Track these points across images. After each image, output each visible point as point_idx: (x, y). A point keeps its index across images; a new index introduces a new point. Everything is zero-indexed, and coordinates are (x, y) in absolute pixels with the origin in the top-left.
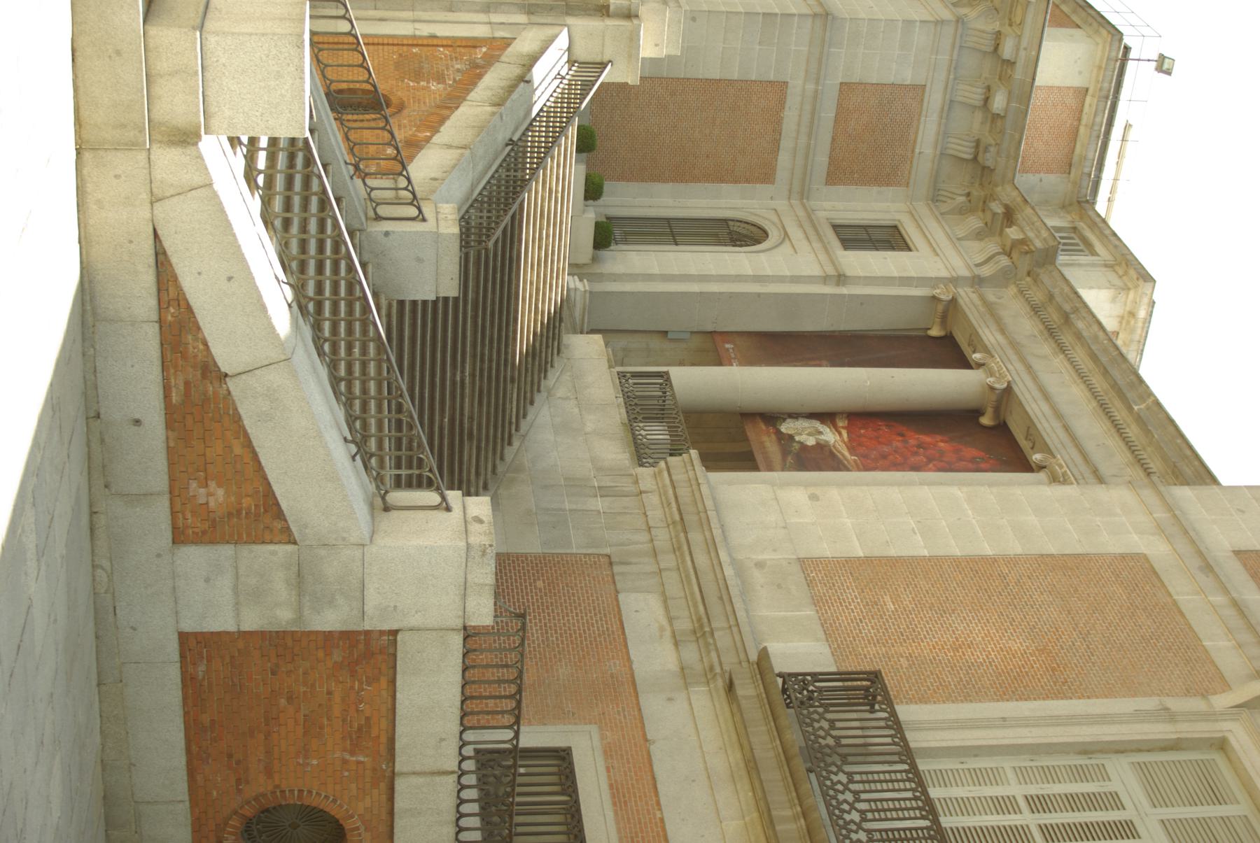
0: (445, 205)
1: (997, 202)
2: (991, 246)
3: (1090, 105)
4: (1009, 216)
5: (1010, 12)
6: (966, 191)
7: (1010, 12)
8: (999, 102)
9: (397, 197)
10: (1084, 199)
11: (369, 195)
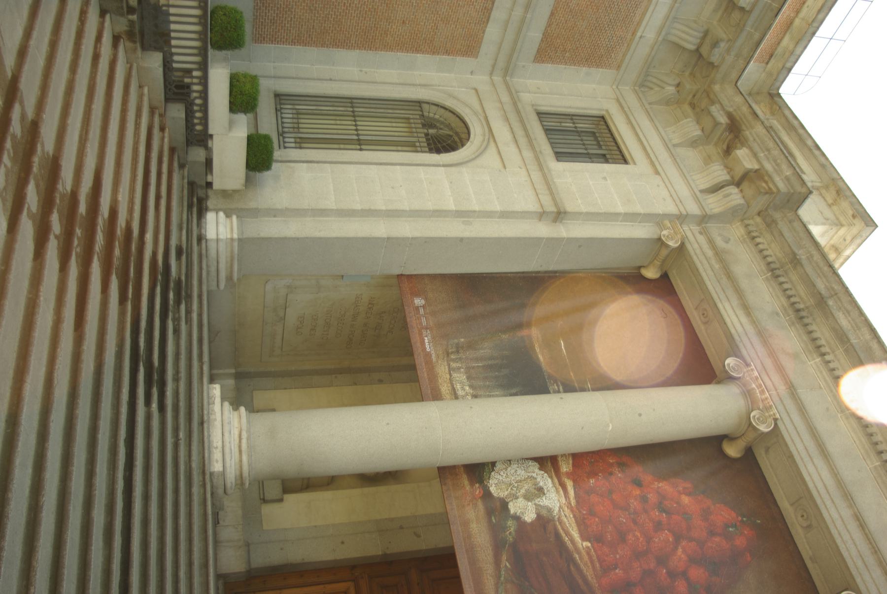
1: (718, 106)
6: (676, 82)
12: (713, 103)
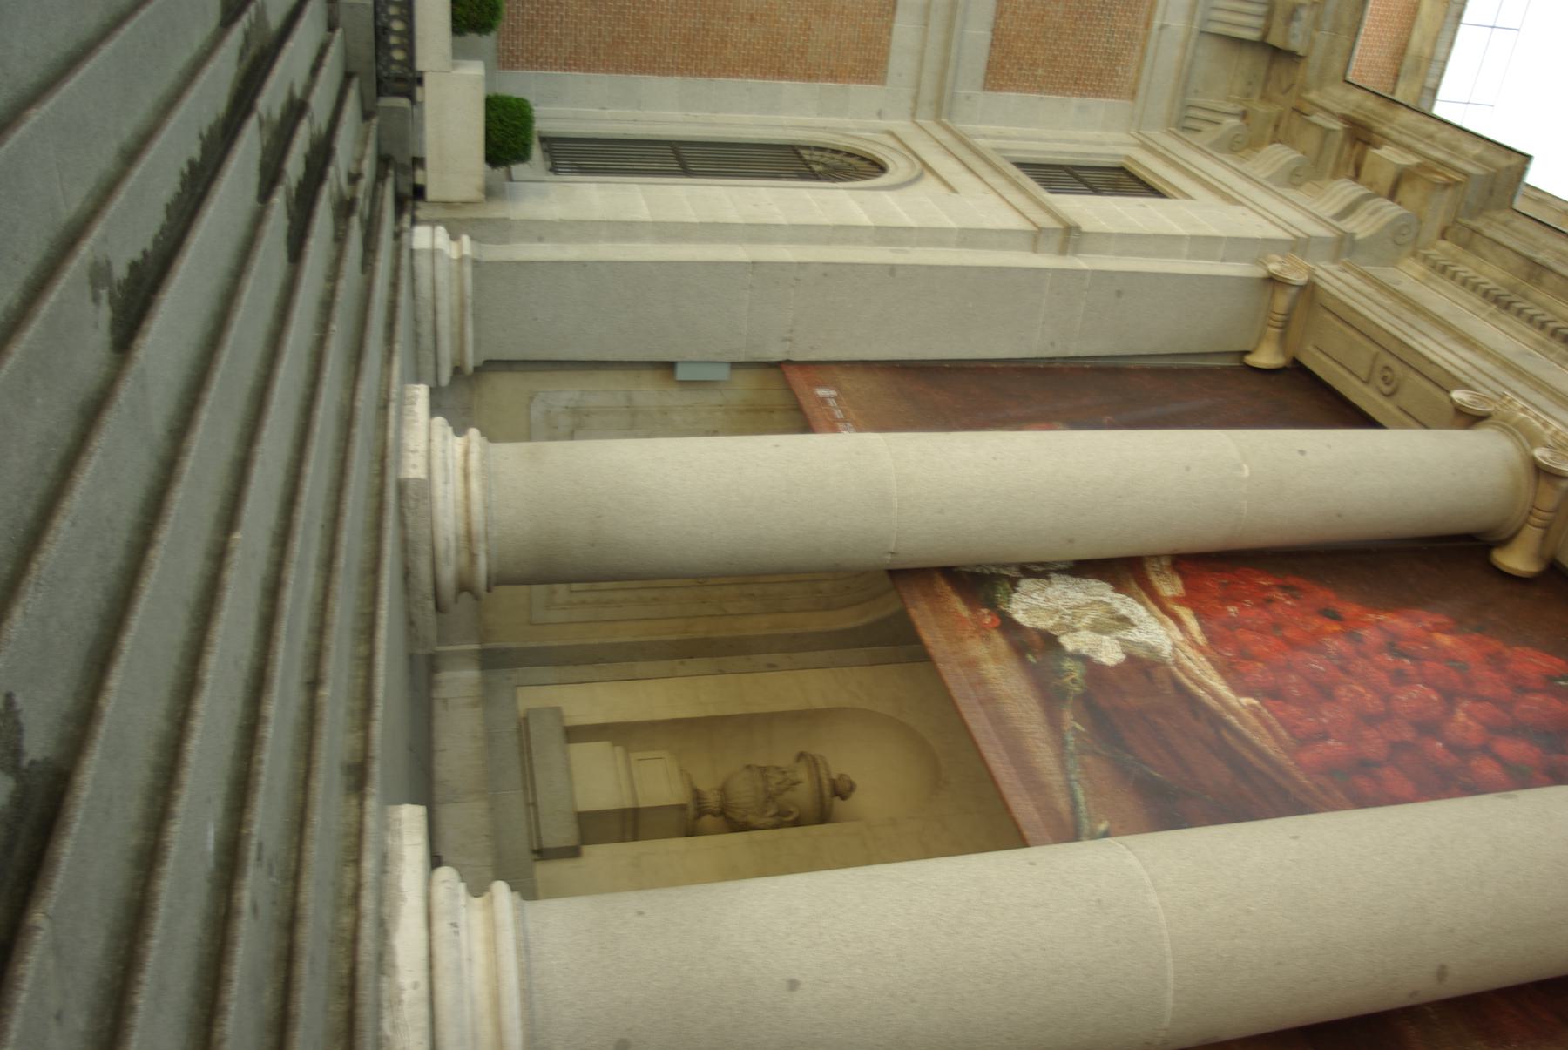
2: (1346, 190)
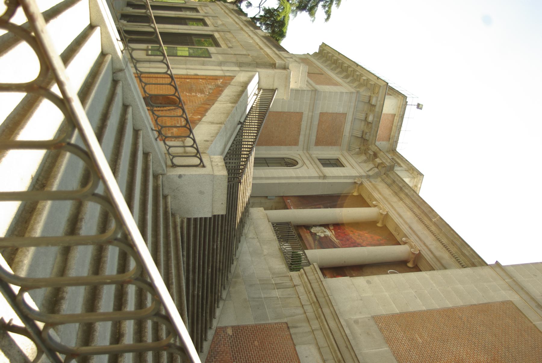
0: (216, 157)
1: (370, 151)
2: (371, 165)
3: (396, 120)
4: (375, 155)
5: (373, 90)
6: (359, 147)
7: (373, 90)
8: (370, 119)
9: (185, 152)
10: (394, 149)
11: (168, 150)
12: (369, 150)
